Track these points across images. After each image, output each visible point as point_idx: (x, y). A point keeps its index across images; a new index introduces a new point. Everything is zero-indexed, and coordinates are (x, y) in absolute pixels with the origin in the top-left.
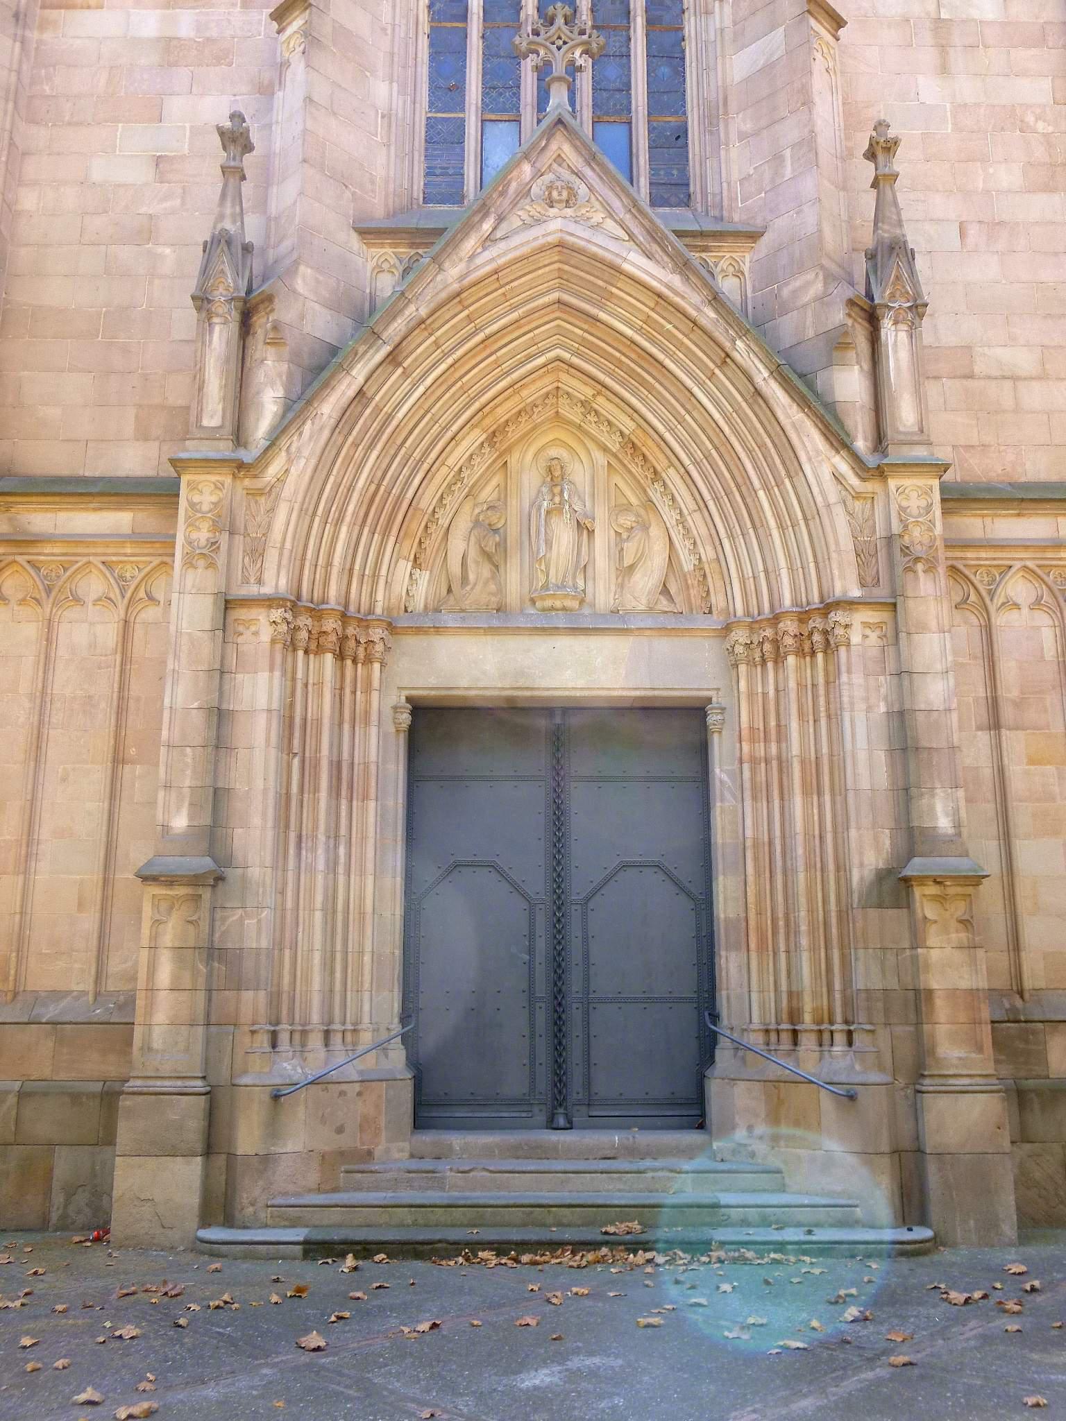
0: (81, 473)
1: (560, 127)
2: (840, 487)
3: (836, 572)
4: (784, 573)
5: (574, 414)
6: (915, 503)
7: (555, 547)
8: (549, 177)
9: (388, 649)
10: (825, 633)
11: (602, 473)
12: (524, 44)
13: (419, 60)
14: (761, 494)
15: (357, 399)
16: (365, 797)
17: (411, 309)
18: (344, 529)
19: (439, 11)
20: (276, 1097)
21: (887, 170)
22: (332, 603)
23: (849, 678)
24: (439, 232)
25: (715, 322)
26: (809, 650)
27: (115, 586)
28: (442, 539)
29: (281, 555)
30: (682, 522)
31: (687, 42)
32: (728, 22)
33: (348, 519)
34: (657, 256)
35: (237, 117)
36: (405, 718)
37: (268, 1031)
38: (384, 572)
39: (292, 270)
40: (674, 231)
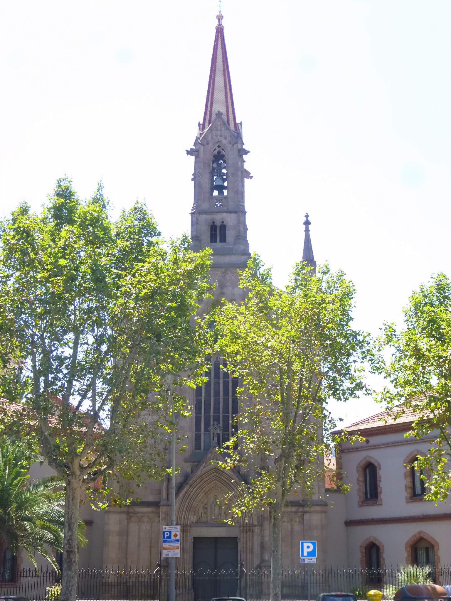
16: (187, 553)
36: (193, 541)
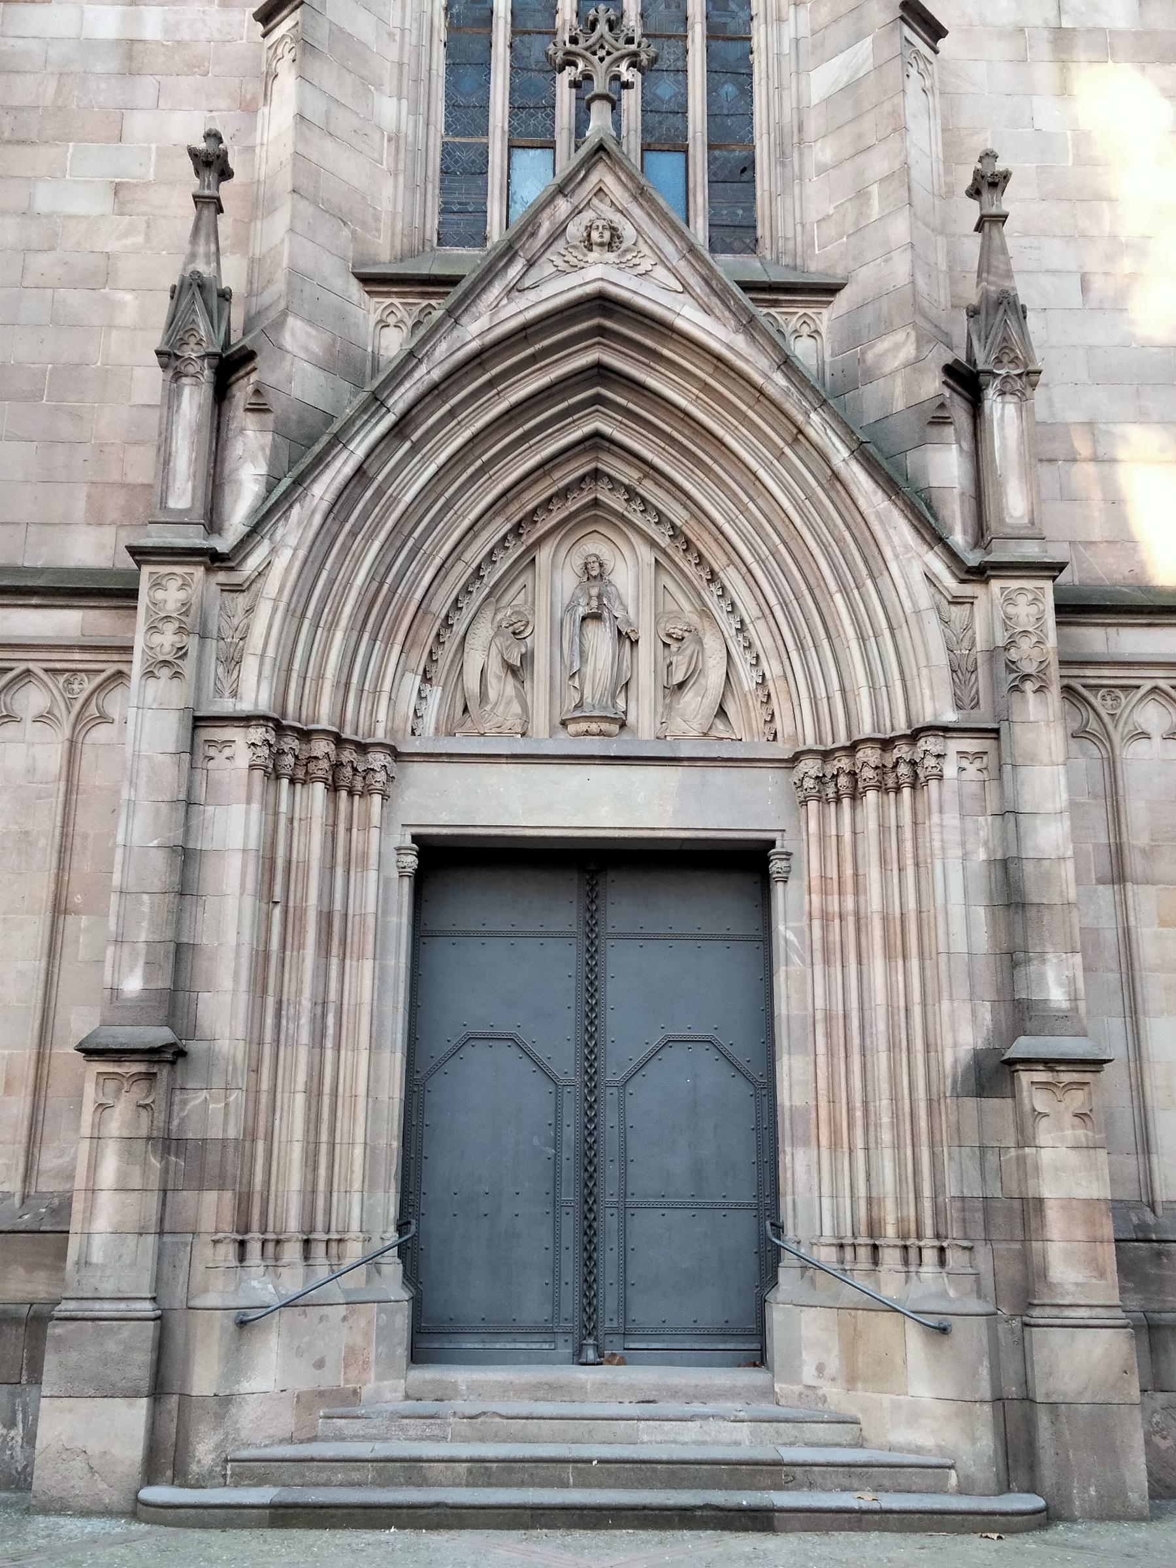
0: (20, 563)
1: (602, 154)
2: (932, 589)
3: (927, 692)
4: (864, 693)
5: (616, 501)
6: (1023, 611)
7: (591, 660)
8: (588, 215)
9: (390, 779)
10: (913, 763)
11: (649, 572)
12: (560, 54)
13: (434, 72)
14: (838, 598)
15: (356, 479)
16: (361, 957)
17: (423, 369)
18: (339, 635)
19: (458, 15)
20: (242, 1324)
21: (994, 210)
22: (324, 724)
23: (941, 819)
24: (453, 281)
25: (787, 393)
26: (894, 785)
27: (59, 698)
28: (457, 650)
29: (261, 664)
30: (742, 629)
31: (755, 55)
32: (804, 31)
33: (343, 622)
34: (717, 311)
35: (213, 136)
36: (411, 861)
37: (235, 1240)
38: (387, 686)
39: (279, 324)
40: (738, 283)
